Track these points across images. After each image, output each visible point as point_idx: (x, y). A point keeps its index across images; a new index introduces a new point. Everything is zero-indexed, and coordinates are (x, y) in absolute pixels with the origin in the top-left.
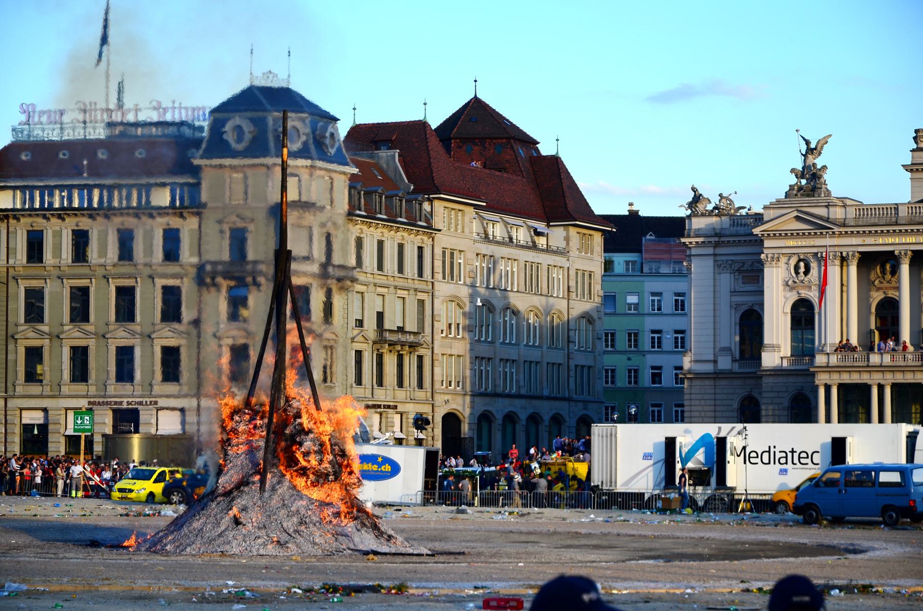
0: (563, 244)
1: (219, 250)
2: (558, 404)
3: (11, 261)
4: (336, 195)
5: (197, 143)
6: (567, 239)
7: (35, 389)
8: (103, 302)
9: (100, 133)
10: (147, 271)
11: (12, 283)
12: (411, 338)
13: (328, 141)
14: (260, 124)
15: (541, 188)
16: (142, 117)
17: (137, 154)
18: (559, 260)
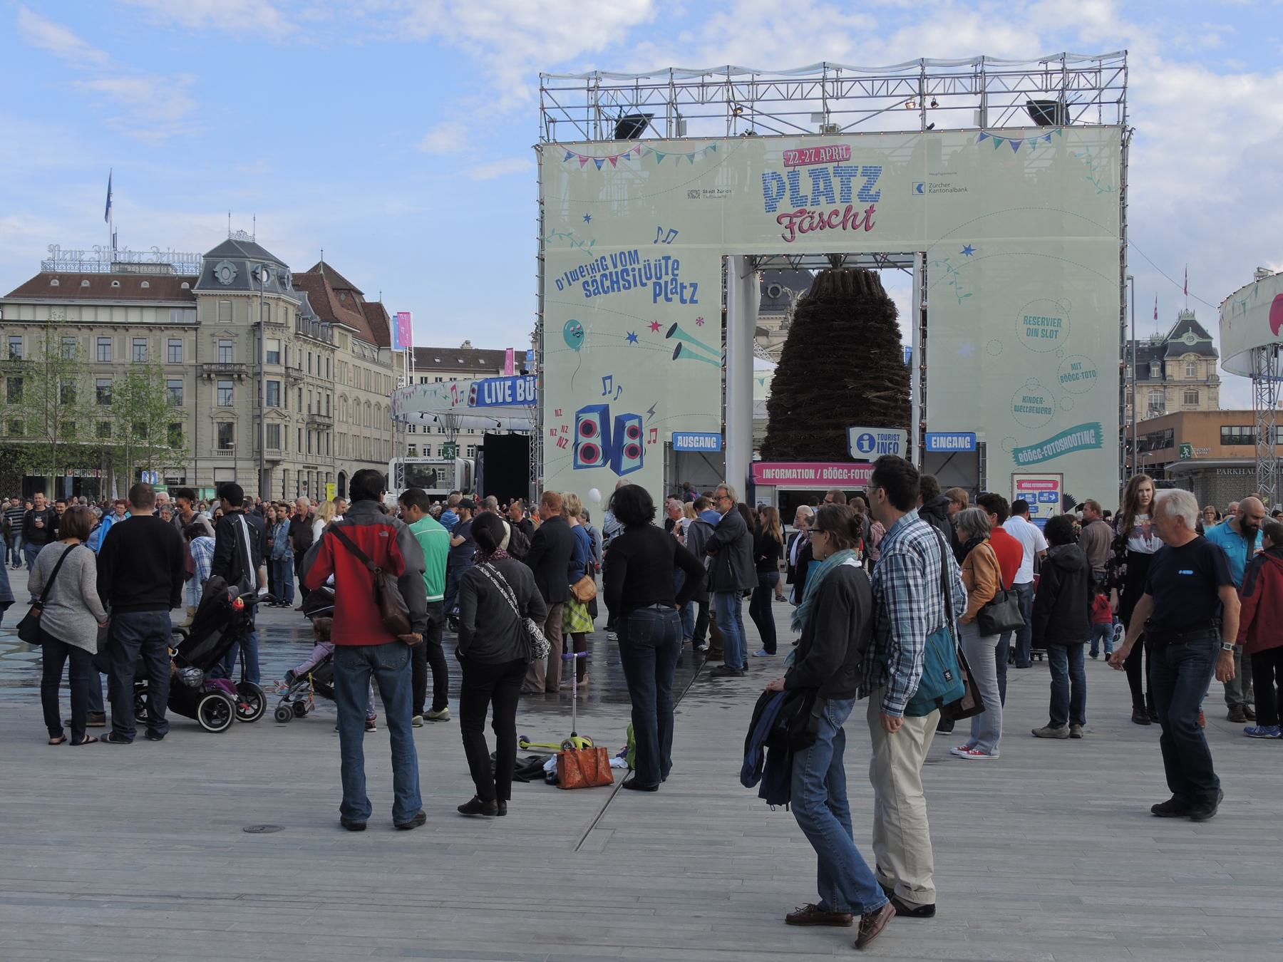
12: (327, 421)
14: (241, 266)
15: (376, 324)
16: (144, 259)
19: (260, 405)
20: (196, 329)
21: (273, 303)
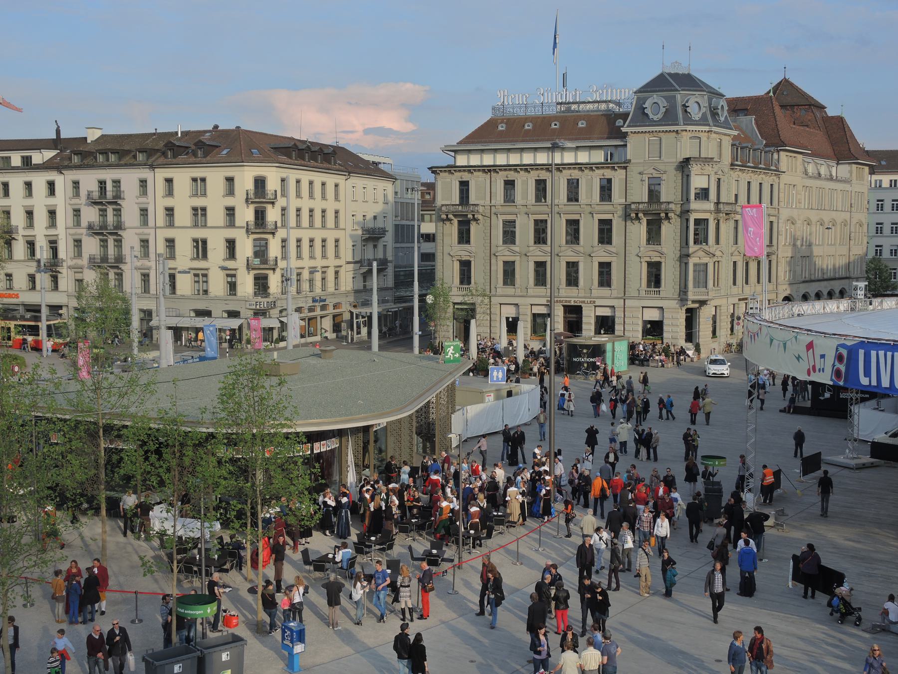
0: (848, 176)
1: (640, 194)
2: (843, 281)
3: (493, 202)
4: (723, 151)
5: (624, 116)
6: (851, 172)
7: (509, 290)
8: (558, 231)
9: (552, 111)
10: (589, 209)
11: (494, 217)
13: (719, 111)
14: (671, 100)
17: (580, 125)
18: (847, 187)
19: (687, 243)
20: (625, 168)
21: (704, 136)
